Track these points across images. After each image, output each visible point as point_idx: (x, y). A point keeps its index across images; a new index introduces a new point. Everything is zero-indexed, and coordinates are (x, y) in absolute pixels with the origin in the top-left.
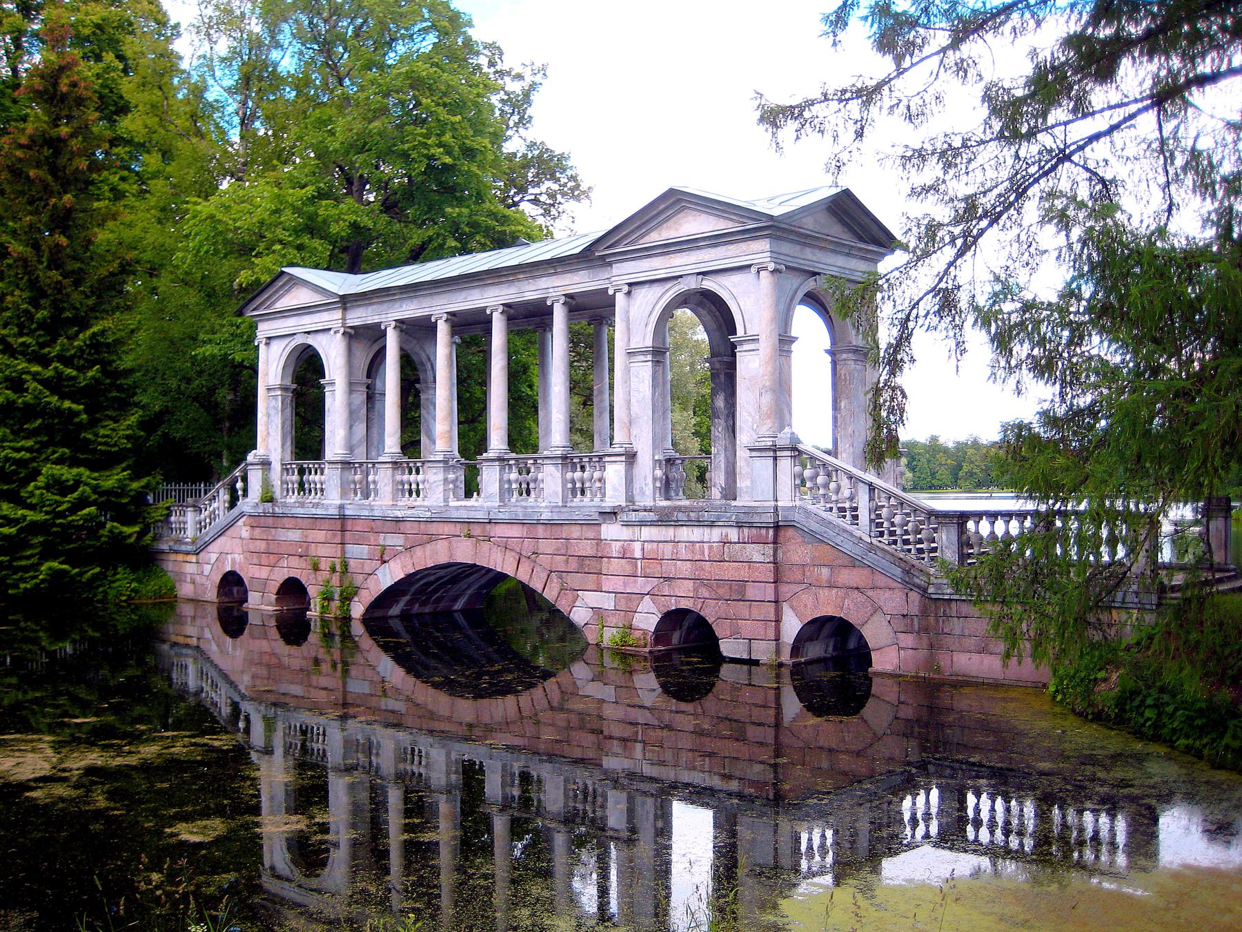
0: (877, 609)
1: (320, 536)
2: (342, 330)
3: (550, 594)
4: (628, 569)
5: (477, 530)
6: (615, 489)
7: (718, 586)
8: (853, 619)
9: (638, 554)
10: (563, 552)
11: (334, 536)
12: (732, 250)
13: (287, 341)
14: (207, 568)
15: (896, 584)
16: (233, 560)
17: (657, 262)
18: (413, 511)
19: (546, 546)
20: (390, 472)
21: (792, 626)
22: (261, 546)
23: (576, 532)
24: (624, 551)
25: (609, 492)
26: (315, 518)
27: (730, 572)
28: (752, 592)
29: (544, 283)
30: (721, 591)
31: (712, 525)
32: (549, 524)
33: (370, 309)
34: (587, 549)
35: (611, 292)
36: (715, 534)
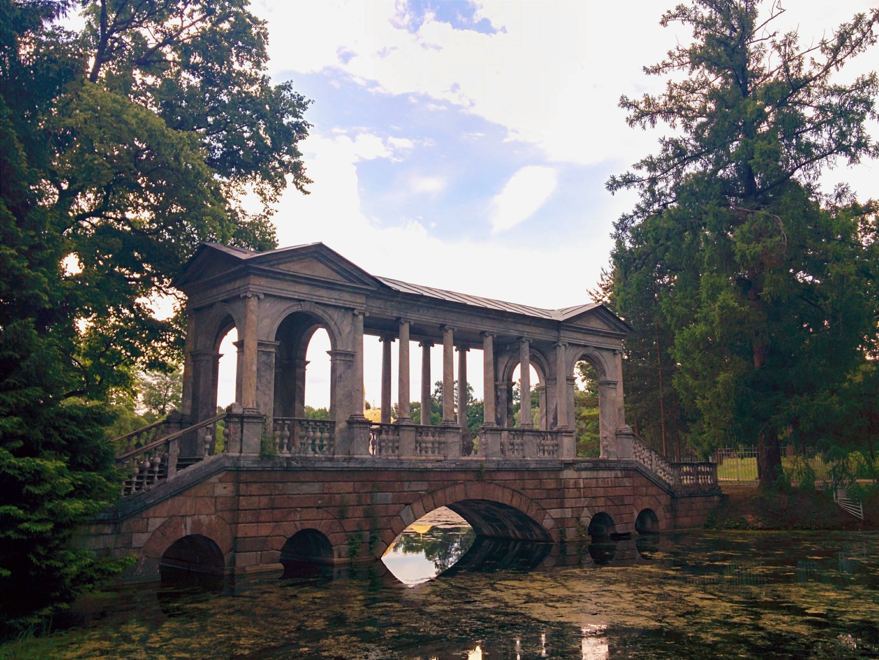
2: (367, 314)
3: (532, 514)
6: (568, 451)
8: (653, 509)
9: (582, 486)
10: (539, 487)
12: (609, 340)
14: (140, 539)
15: (663, 492)
16: (197, 524)
17: (580, 336)
18: (440, 464)
19: (530, 484)
20: (413, 434)
21: (636, 514)
22: (265, 501)
24: (576, 483)
25: (565, 452)
26: (342, 471)
27: (619, 492)
29: (520, 327)
31: (613, 469)
32: (534, 471)
33: (389, 304)
34: (551, 484)
35: (560, 344)
36: (612, 474)
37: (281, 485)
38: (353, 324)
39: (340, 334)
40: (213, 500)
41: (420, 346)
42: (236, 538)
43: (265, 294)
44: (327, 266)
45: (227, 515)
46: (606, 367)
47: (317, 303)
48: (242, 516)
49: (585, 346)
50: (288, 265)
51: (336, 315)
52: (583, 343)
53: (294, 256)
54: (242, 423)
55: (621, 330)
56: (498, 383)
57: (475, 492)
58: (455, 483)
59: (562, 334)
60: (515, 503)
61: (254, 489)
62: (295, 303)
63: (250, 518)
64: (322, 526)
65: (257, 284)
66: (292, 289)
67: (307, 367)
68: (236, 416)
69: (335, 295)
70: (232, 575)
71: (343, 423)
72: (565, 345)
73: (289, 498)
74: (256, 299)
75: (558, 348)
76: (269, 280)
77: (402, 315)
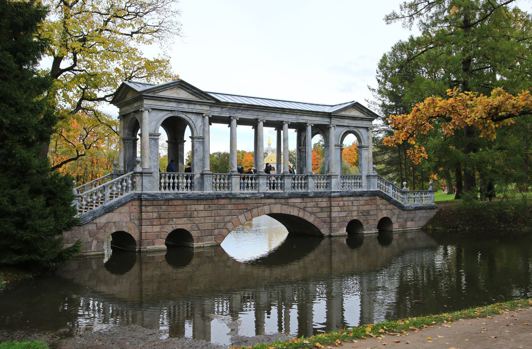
0: (394, 214)
1: (201, 207)
4: (340, 210)
5: (283, 201)
6: (335, 186)
7: (364, 212)
10: (316, 206)
11: (210, 207)
13: (166, 113)
19: (310, 204)
22: (155, 215)
23: (320, 200)
28: (371, 213)
30: (364, 213)
33: (223, 110)
35: (331, 126)
37: (164, 207)
38: (203, 121)
39: (196, 128)
40: (129, 215)
41: (253, 128)
42: (142, 233)
43: (152, 109)
44: (186, 91)
45: (137, 222)
46: (361, 138)
47: (181, 111)
48: (144, 222)
49: (348, 126)
50: (164, 92)
51: (193, 117)
52: (346, 124)
53: (167, 87)
54: (142, 176)
55: (372, 116)
56: (301, 148)
57: (277, 209)
58: (264, 204)
59: (332, 121)
60: (301, 215)
61: (149, 209)
62: (169, 112)
63: (148, 223)
64: (187, 227)
65: (147, 103)
66: (167, 105)
67: (185, 143)
68: (138, 173)
69: (192, 106)
70: (140, 252)
71: (198, 175)
72: (334, 127)
73: (169, 213)
74: (147, 111)
75: (330, 129)
76: (154, 101)
77: (232, 115)
